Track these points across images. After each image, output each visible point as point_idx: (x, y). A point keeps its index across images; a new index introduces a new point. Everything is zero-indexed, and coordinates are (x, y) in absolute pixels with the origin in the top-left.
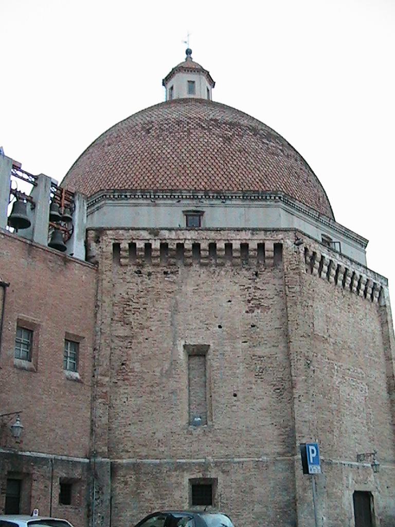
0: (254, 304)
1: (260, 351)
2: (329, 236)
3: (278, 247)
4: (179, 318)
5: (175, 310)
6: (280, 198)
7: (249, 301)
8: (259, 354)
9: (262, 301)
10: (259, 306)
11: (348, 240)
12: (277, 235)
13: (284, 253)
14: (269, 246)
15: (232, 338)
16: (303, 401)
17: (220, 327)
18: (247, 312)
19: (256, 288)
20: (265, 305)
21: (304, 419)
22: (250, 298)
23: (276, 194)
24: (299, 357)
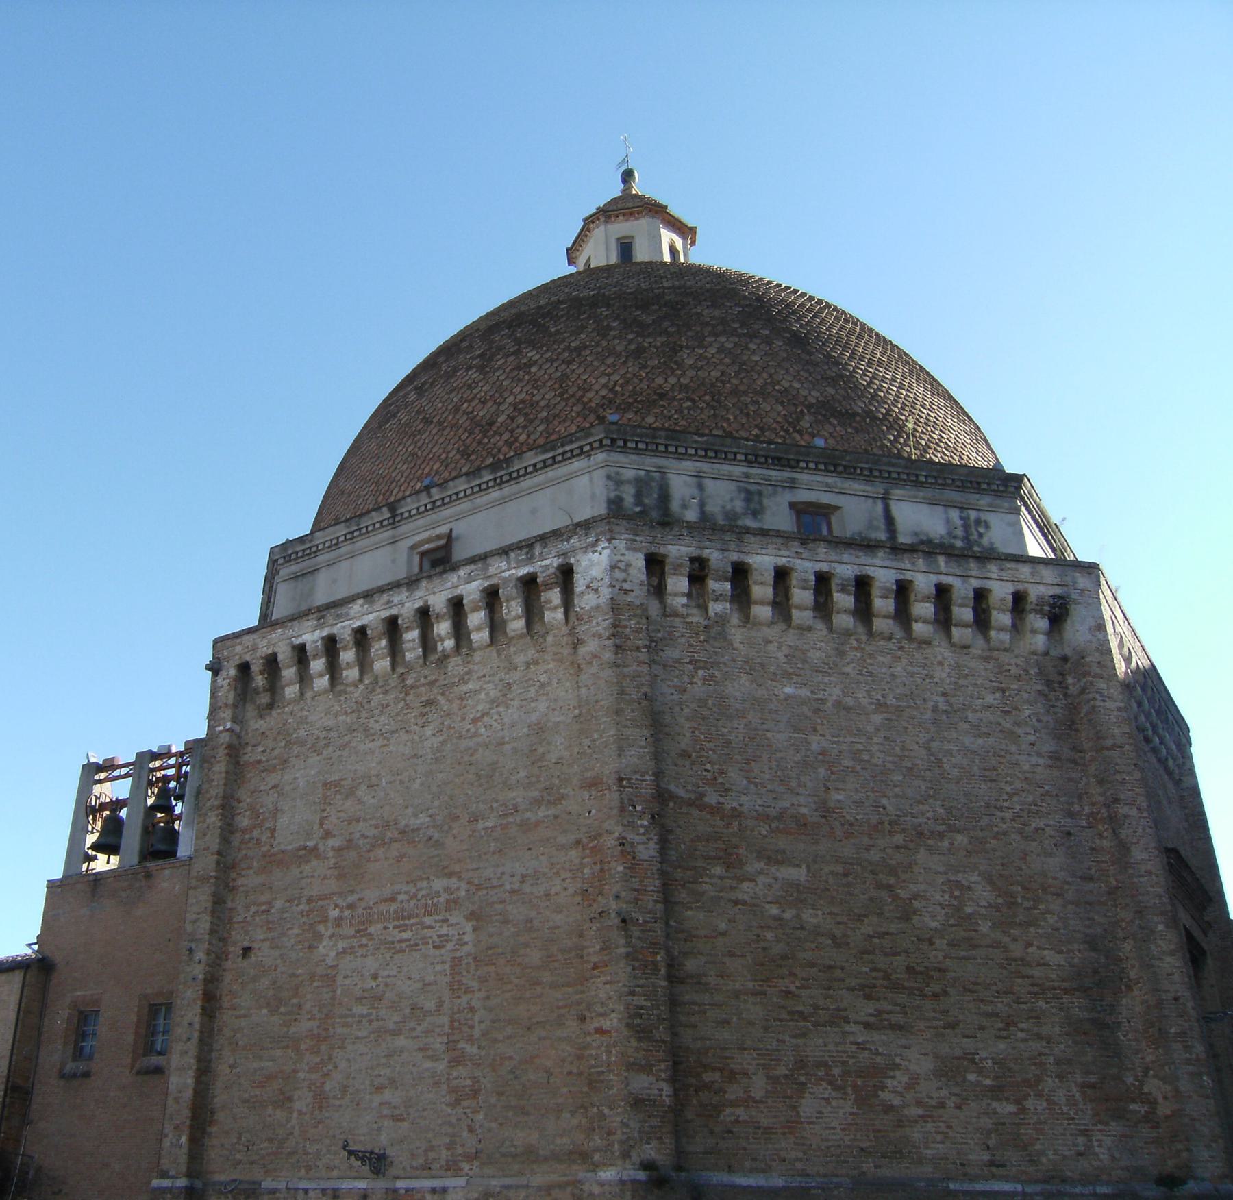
11: (526, 483)
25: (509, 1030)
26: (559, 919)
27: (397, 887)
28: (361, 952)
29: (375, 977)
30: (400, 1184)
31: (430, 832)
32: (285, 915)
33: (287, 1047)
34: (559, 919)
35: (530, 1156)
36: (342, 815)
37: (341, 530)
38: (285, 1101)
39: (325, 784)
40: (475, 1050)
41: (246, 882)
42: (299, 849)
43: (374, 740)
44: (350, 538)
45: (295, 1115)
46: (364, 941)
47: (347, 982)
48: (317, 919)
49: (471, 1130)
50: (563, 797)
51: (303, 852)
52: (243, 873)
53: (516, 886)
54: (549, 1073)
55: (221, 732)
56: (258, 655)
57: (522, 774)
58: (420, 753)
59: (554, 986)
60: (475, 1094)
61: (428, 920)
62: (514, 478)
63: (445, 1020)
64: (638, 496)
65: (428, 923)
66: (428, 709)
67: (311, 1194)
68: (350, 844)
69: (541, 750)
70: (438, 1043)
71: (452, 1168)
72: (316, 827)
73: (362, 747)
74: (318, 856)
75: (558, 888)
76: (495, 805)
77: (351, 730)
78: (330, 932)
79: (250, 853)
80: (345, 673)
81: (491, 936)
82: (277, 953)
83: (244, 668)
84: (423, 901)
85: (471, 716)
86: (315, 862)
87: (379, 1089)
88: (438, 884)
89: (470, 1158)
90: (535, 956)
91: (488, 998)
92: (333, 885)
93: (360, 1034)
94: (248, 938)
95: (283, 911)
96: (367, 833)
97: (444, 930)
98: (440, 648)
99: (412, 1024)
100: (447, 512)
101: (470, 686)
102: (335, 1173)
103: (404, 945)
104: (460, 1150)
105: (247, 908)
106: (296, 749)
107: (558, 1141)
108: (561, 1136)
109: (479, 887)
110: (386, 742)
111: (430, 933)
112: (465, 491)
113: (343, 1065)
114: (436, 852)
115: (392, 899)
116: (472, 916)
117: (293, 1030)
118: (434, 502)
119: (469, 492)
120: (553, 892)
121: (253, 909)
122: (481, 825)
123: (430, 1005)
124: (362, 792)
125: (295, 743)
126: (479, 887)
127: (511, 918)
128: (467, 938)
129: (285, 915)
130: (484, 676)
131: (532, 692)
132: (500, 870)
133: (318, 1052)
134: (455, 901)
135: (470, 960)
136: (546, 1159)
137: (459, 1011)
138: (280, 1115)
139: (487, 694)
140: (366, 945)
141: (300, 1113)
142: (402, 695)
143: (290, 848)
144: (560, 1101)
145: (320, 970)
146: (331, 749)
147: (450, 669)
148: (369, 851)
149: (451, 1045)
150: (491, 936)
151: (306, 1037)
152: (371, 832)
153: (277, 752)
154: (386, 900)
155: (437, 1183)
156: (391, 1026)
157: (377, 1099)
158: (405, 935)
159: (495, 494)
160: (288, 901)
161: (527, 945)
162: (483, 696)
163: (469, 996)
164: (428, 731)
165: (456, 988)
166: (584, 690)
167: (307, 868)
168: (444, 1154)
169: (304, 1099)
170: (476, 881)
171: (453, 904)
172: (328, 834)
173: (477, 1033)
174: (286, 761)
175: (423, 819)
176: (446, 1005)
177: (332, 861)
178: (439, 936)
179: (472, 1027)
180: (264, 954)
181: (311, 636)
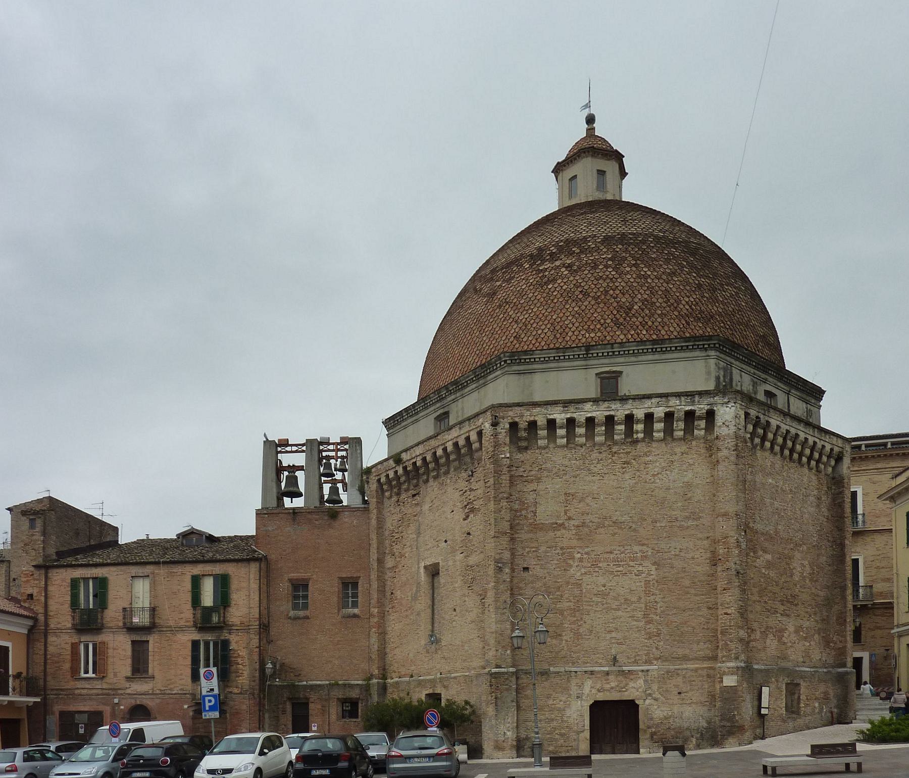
0: (470, 510)
1: (473, 560)
2: (615, 369)
3: (480, 434)
4: (421, 539)
5: (419, 534)
6: (505, 361)
7: (466, 506)
8: (471, 563)
9: (474, 503)
10: (472, 510)
12: (478, 420)
13: (483, 442)
14: (474, 437)
15: (453, 551)
16: (491, 610)
17: (446, 541)
18: (464, 519)
19: (471, 490)
20: (477, 507)
21: (491, 630)
22: (465, 503)
23: (500, 358)
24: (490, 563)
25: (675, 611)
26: (698, 568)
27: (613, 548)
28: (595, 574)
29: (604, 586)
30: (624, 668)
31: (631, 524)
32: (548, 554)
33: (556, 613)
34: (698, 568)
35: (685, 659)
36: (578, 510)
37: (553, 354)
38: (558, 636)
39: (566, 494)
40: (658, 618)
41: (520, 536)
42: (553, 524)
43: (594, 476)
44: (557, 360)
45: (564, 642)
46: (597, 569)
47: (589, 587)
48: (567, 557)
49: (657, 648)
50: (700, 517)
51: (556, 525)
52: (518, 531)
53: (677, 553)
54: (694, 628)
55: (502, 458)
56: (524, 419)
57: (680, 504)
58: (623, 486)
59: (696, 595)
60: (659, 635)
61: (632, 563)
62: (663, 352)
63: (643, 606)
64: (724, 376)
65: (632, 565)
66: (625, 466)
67: (579, 673)
68: (583, 524)
69: (689, 495)
70: (639, 615)
71: (648, 662)
72: (563, 514)
73: (588, 478)
74: (565, 528)
75: (698, 556)
76: (665, 517)
77: (579, 469)
78: (576, 564)
79: (521, 522)
80: (577, 439)
81: (665, 573)
82: (546, 571)
83: (514, 426)
84: (628, 555)
85: (652, 473)
86: (564, 531)
87: (610, 632)
88: (636, 548)
89: (657, 659)
90: (687, 583)
91: (664, 598)
92: (574, 543)
93: (597, 609)
94: (526, 563)
95: (546, 552)
96: (593, 521)
97: (640, 568)
98: (635, 436)
99: (626, 607)
100: (622, 360)
101: (650, 458)
102: (588, 665)
103: (619, 573)
104: (652, 656)
105: (523, 548)
106: (545, 473)
107: (698, 653)
108: (699, 651)
109: (658, 552)
110: (601, 478)
111: (632, 569)
112: (634, 350)
113: (589, 622)
114: (634, 534)
115: (611, 553)
116: (654, 564)
117: (558, 606)
118: (614, 352)
119: (636, 351)
120: (696, 557)
121: (527, 550)
122: (658, 524)
123: (634, 599)
124: (589, 500)
125: (544, 470)
126: (658, 552)
127: (675, 566)
128: (652, 573)
129: (548, 554)
130: (658, 455)
131: (684, 467)
132: (669, 546)
133: (574, 616)
134: (645, 557)
135: (654, 582)
136: (692, 659)
137: (649, 603)
138: (554, 641)
139: (660, 464)
140: (598, 572)
141: (567, 641)
142: (610, 456)
143: (547, 522)
144: (699, 638)
145: (572, 581)
146: (567, 477)
147: (638, 447)
148: (595, 529)
149: (645, 616)
150: (665, 573)
151: (567, 610)
152: (596, 520)
153: (533, 473)
154: (607, 553)
155: (645, 668)
156: (614, 607)
157: (608, 636)
158: (619, 569)
159: (650, 357)
160: (549, 548)
161: (683, 578)
162: (658, 464)
163: (655, 596)
164: (627, 476)
165: (647, 593)
166: (720, 473)
167: (558, 533)
168: (644, 657)
169: (567, 636)
170: (657, 549)
171: (644, 557)
172: (570, 518)
173: (659, 611)
174: (540, 479)
175: (626, 518)
176: (643, 600)
177: (574, 531)
178: (638, 571)
179: (656, 609)
180: (537, 571)
181: (560, 416)
